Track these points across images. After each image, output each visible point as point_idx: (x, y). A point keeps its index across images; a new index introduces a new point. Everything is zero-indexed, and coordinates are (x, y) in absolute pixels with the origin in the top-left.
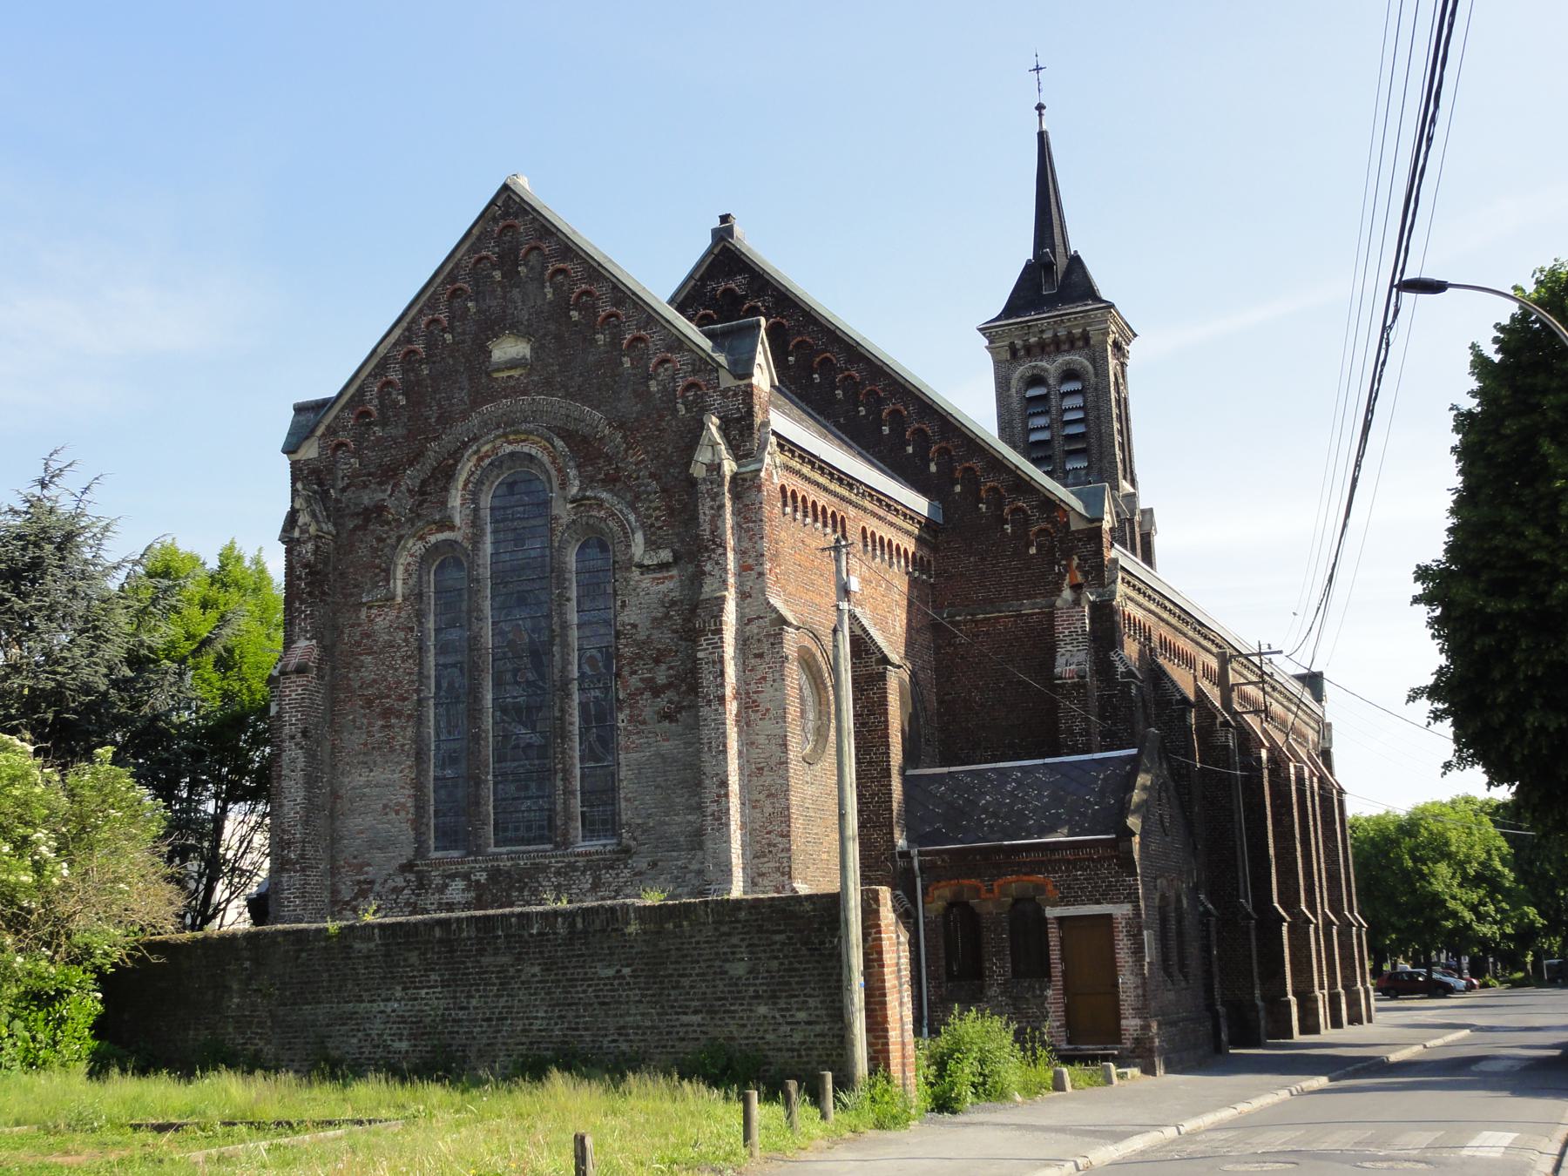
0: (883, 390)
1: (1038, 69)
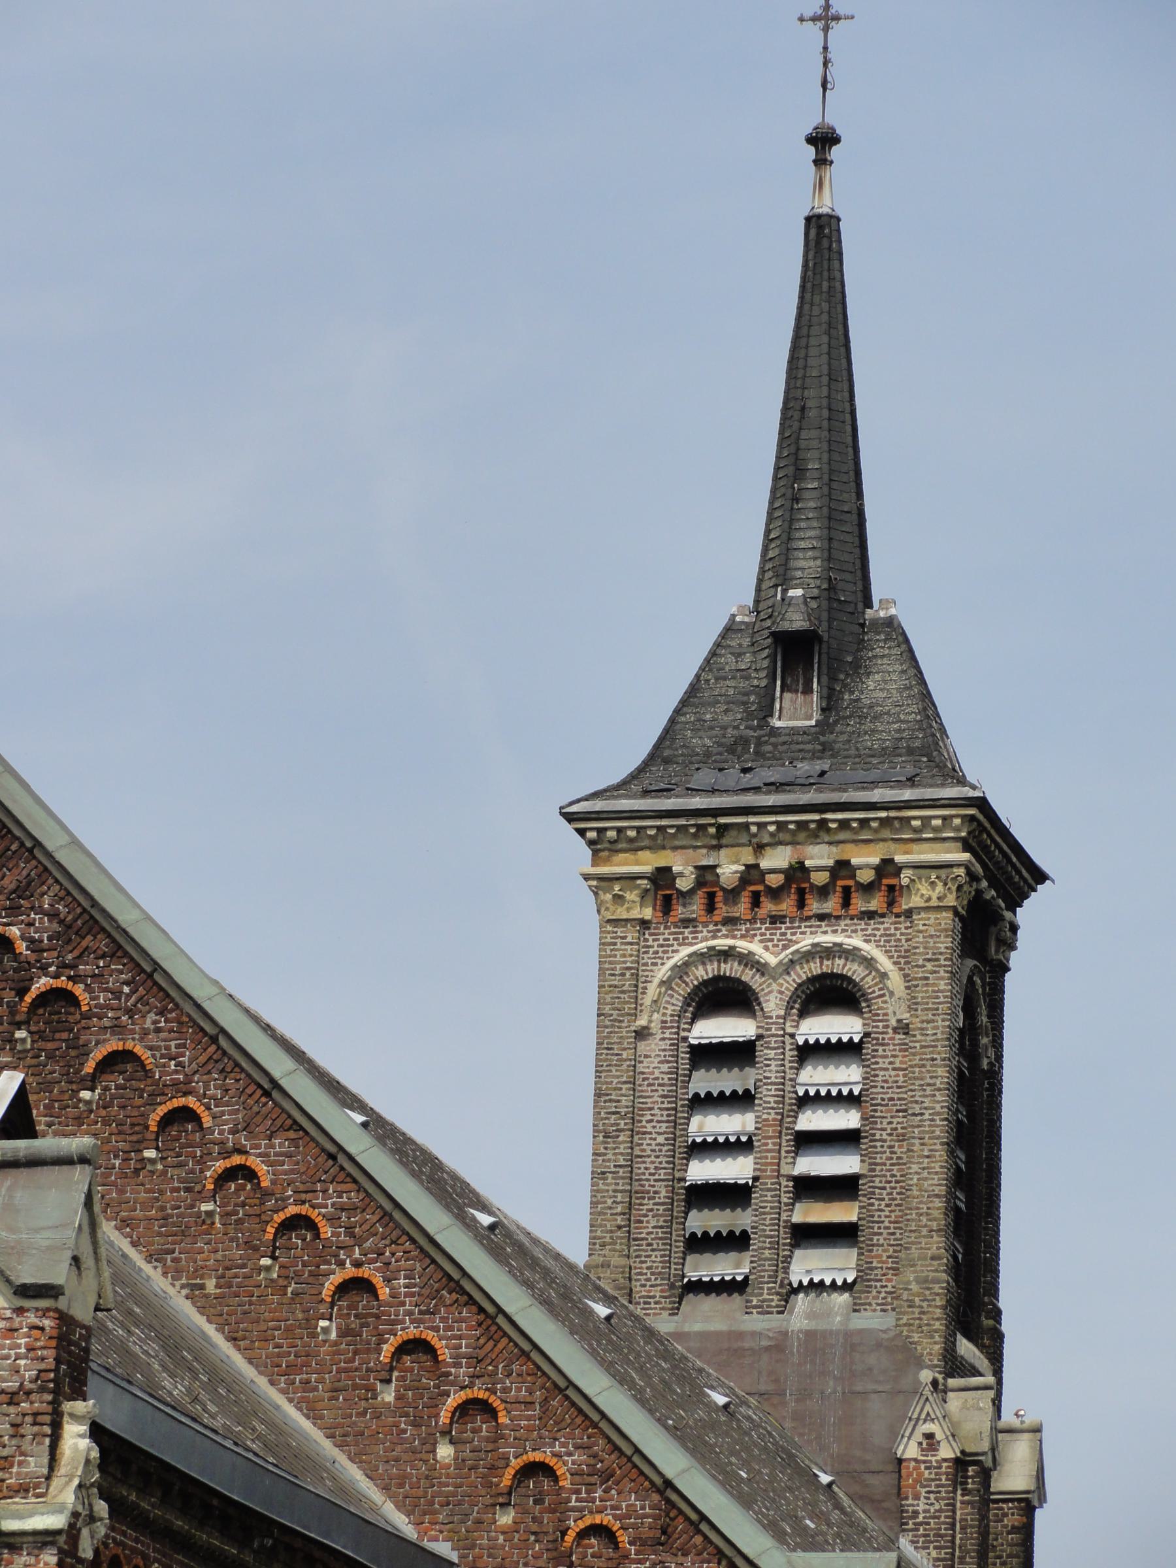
0: (332, 1220)
1: (827, 18)
